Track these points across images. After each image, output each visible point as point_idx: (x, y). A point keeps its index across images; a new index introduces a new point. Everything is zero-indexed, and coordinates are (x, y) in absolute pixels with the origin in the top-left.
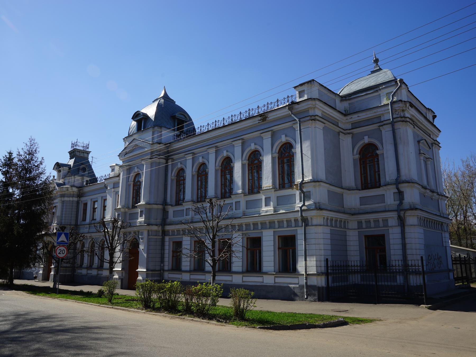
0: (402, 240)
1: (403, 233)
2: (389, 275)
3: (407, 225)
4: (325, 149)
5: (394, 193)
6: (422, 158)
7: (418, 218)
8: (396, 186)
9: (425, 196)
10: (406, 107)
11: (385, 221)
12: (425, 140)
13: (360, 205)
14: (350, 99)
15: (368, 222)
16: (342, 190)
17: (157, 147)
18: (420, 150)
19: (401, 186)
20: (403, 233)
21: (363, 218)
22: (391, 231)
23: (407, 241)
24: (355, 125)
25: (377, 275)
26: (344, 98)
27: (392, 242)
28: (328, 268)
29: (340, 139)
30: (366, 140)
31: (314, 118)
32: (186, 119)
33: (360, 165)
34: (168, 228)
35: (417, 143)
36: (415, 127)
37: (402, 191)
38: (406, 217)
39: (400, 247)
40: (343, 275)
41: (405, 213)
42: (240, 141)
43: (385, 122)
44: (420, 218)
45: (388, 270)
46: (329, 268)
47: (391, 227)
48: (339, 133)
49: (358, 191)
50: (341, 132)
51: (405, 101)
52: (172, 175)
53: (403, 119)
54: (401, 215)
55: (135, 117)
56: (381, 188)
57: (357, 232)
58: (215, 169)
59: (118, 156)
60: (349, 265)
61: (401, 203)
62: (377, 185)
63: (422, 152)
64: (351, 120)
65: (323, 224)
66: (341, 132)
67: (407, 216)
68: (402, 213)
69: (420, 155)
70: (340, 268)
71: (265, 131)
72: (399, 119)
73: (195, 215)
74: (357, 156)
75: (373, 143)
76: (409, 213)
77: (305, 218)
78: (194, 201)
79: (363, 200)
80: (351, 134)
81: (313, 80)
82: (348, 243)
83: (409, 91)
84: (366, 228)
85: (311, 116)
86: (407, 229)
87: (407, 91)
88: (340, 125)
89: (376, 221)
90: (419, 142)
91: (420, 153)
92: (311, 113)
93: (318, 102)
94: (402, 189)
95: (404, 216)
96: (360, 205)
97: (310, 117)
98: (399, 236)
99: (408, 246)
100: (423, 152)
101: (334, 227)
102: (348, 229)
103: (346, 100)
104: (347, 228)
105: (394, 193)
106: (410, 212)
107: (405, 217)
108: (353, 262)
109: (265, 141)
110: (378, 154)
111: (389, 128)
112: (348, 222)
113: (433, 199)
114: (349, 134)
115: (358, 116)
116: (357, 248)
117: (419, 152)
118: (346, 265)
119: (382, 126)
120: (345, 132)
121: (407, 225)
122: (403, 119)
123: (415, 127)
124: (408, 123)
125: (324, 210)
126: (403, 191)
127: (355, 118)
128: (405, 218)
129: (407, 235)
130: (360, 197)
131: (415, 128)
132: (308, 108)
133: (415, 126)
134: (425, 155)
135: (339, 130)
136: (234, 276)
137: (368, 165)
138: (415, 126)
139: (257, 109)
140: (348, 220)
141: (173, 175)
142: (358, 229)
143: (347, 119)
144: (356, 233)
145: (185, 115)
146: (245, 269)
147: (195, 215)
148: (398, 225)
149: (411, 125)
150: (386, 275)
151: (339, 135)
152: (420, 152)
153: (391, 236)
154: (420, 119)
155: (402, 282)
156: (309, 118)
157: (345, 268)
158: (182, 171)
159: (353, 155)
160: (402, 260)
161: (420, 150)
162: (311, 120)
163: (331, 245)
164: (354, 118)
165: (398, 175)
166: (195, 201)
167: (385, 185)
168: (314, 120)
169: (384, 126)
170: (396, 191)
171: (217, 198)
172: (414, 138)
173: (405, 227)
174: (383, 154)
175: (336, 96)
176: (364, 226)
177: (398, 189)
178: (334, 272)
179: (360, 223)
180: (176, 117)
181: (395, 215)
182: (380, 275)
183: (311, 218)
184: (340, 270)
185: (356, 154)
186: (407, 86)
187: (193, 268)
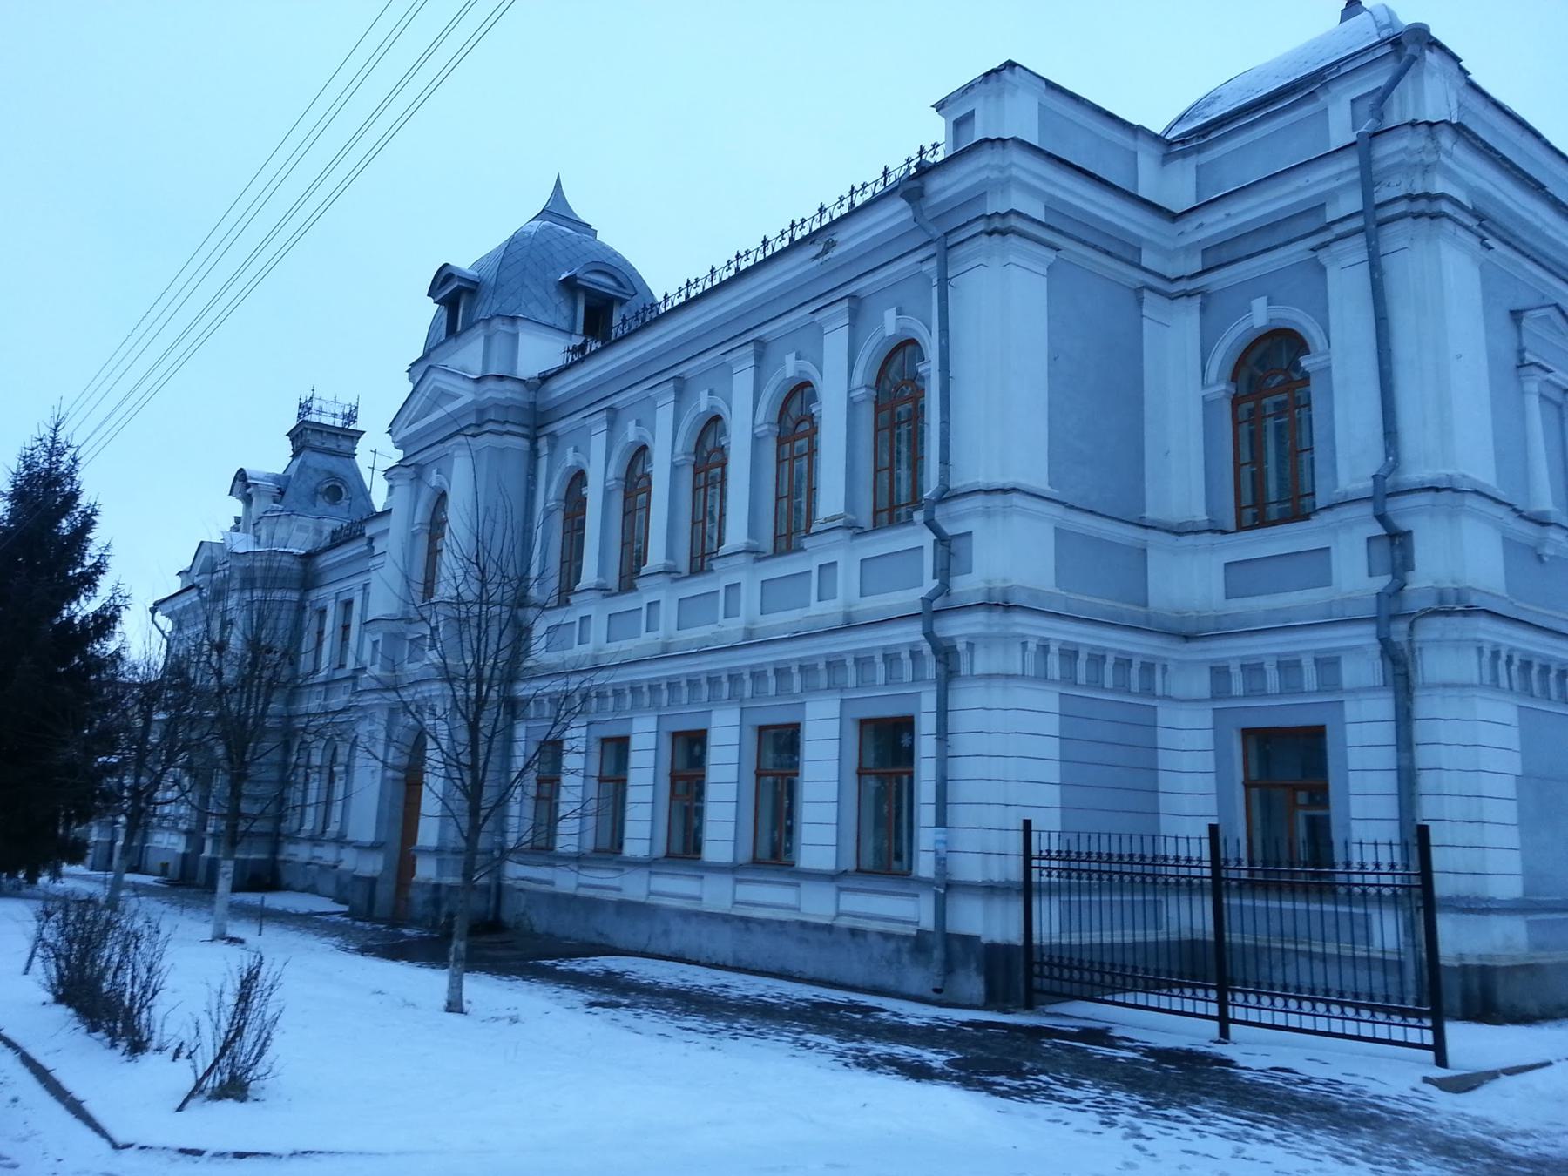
0: (1398, 750)
1: (1404, 718)
2: (1343, 909)
3: (1423, 683)
4: (1053, 359)
5: (1369, 540)
6: (1532, 387)
7: (1480, 651)
8: (1375, 508)
9: (1540, 558)
10: (1438, 149)
11: (1328, 664)
12: (1557, 306)
13: (1227, 598)
14: (1199, 150)
15: (1253, 669)
16: (1138, 533)
17: (493, 391)
18: (1521, 351)
19: (1393, 506)
20: (1404, 718)
21: (1233, 651)
22: (1351, 710)
23: (1423, 756)
24: (1218, 255)
25: (1225, 901)
26: (1179, 147)
27: (1355, 758)
28: (1030, 864)
29: (1145, 322)
30: (1260, 315)
31: (1001, 227)
32: (621, 289)
33: (1236, 423)
34: (523, 690)
35: (1504, 321)
36: (1491, 242)
37: (1406, 529)
38: (1420, 649)
39: (1389, 782)
40: (1103, 898)
41: (1411, 628)
42: (751, 348)
43: (1339, 229)
44: (1496, 654)
45: (1342, 890)
46: (1035, 863)
47: (1352, 691)
48: (1138, 292)
49: (1218, 538)
50: (1152, 289)
51: (1430, 125)
52: (549, 493)
53: (1421, 205)
54: (1395, 638)
55: (441, 286)
56: (1315, 521)
57: (1209, 714)
58: (672, 463)
59: (389, 432)
60: (1166, 858)
61: (1397, 590)
62: (1298, 508)
63: (1529, 357)
64: (1201, 235)
65: (1020, 673)
66: (1152, 289)
67: (1423, 641)
68: (1399, 630)
69: (1524, 371)
70: (1105, 867)
71: (822, 300)
72: (1401, 207)
73: (608, 642)
74: (1221, 389)
75: (1288, 326)
76: (1432, 629)
77: (945, 644)
78: (606, 590)
79: (1239, 576)
80: (1199, 296)
81: (1010, 65)
82: (1164, 760)
83: (1473, 86)
84: (1245, 696)
85: (989, 217)
86: (1424, 705)
87: (1462, 83)
88: (1148, 260)
89: (1288, 666)
90: (1516, 315)
91: (1521, 365)
92: (995, 205)
93: (1018, 157)
94: (1403, 524)
95: (1410, 641)
96: (1227, 598)
97: (984, 220)
98: (1386, 733)
99: (1426, 782)
100: (1535, 360)
101: (1082, 686)
102: (1167, 698)
103: (1184, 154)
104: (1159, 691)
105: (1369, 540)
106: (1438, 622)
107: (1417, 645)
108: (1182, 843)
109: (829, 341)
110: (1308, 372)
111: (1354, 250)
112: (1165, 667)
113: (1546, 559)
114: (1188, 295)
115: (1228, 215)
116: (1208, 783)
117: (1514, 362)
118: (1155, 858)
119: (1324, 245)
120: (1173, 290)
121: (1423, 683)
122: (1421, 205)
123: (1491, 242)
124: (1449, 226)
125: (1017, 610)
126: (1410, 533)
127: (1216, 224)
128: (1412, 651)
129: (1420, 731)
130: (1226, 564)
131: (1490, 248)
132: (981, 183)
133: (1486, 235)
134: (1549, 371)
135: (1142, 282)
136: (808, 888)
137: (1270, 424)
138: (1486, 235)
139: (818, 217)
140: (1165, 659)
141: (552, 496)
142: (1214, 698)
143: (1182, 233)
144: (1203, 717)
145: (615, 274)
146: (746, 855)
147: (608, 642)
148: (1385, 685)
149: (1461, 232)
150: (1328, 908)
151: (1140, 302)
152: (1522, 360)
153: (1353, 734)
154: (1530, 212)
155: (1391, 943)
156: (981, 226)
157: (1063, 864)
158: (578, 478)
159: (1204, 385)
160: (1396, 840)
161: (1521, 351)
162: (990, 234)
163: (1060, 761)
164: (1212, 224)
165: (1387, 455)
166: (610, 590)
167: (1329, 507)
168: (1003, 233)
169: (1336, 248)
170: (1378, 530)
171: (673, 575)
172: (1488, 295)
173: (1416, 693)
174: (1328, 368)
175: (1136, 138)
176: (1237, 686)
177: (1382, 518)
178: (1052, 879)
179: (1219, 673)
180: (578, 281)
181: (1365, 636)
182: (1235, 901)
183: (970, 646)
184: (1045, 872)
185: (1218, 381)
186: (1456, 59)
187: (750, 854)
